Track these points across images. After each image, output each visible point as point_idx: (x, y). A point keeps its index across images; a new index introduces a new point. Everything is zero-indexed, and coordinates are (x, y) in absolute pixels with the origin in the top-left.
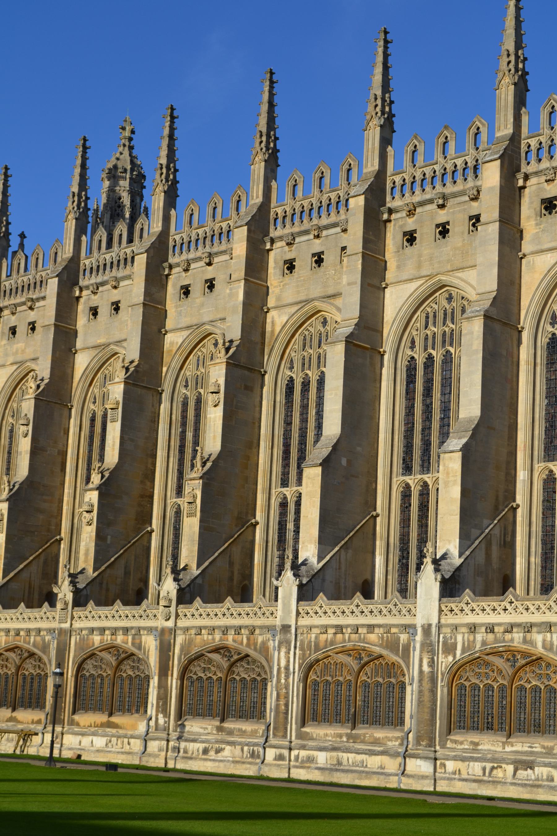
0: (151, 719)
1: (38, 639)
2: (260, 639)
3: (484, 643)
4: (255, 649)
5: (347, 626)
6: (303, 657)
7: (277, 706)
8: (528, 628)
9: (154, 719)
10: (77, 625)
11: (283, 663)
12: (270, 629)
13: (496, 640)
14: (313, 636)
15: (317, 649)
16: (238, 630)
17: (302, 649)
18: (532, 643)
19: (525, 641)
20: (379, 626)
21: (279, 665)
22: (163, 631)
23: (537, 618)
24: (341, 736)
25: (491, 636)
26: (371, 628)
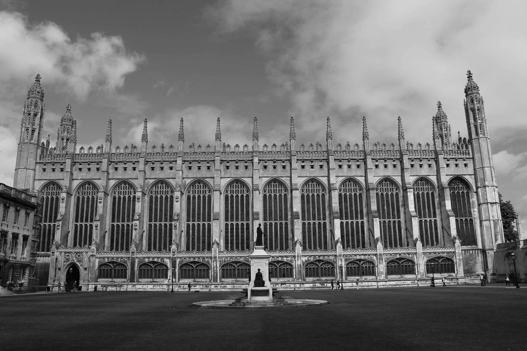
0: (170, 280)
1: (122, 259)
2: (206, 260)
3: (272, 260)
4: (205, 262)
5: (234, 257)
6: (220, 264)
7: (214, 275)
8: (282, 257)
9: (171, 280)
10: (138, 256)
11: (215, 265)
12: (211, 258)
13: (274, 259)
14: (223, 259)
15: (225, 261)
16: (199, 258)
17: (220, 261)
18: (283, 260)
19: (282, 259)
20: (243, 257)
21: (214, 265)
22: (173, 258)
23: (285, 255)
24: (233, 281)
25: (273, 259)
26: (241, 257)
